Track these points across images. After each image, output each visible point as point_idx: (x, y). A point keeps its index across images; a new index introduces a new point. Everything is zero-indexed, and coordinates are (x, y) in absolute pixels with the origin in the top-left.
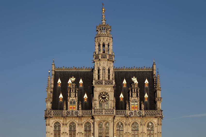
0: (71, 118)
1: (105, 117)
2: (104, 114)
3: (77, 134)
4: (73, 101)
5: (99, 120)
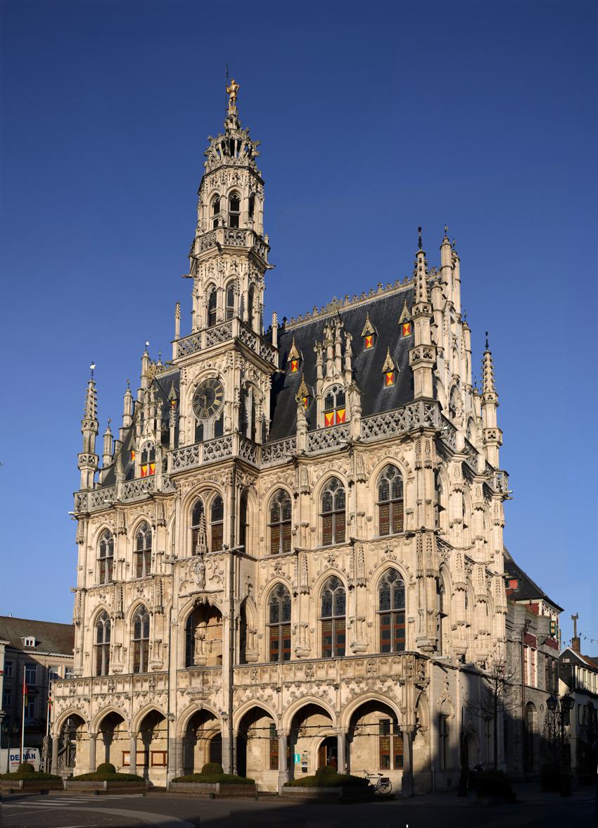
1: (207, 475)
2: (201, 462)
5: (188, 489)
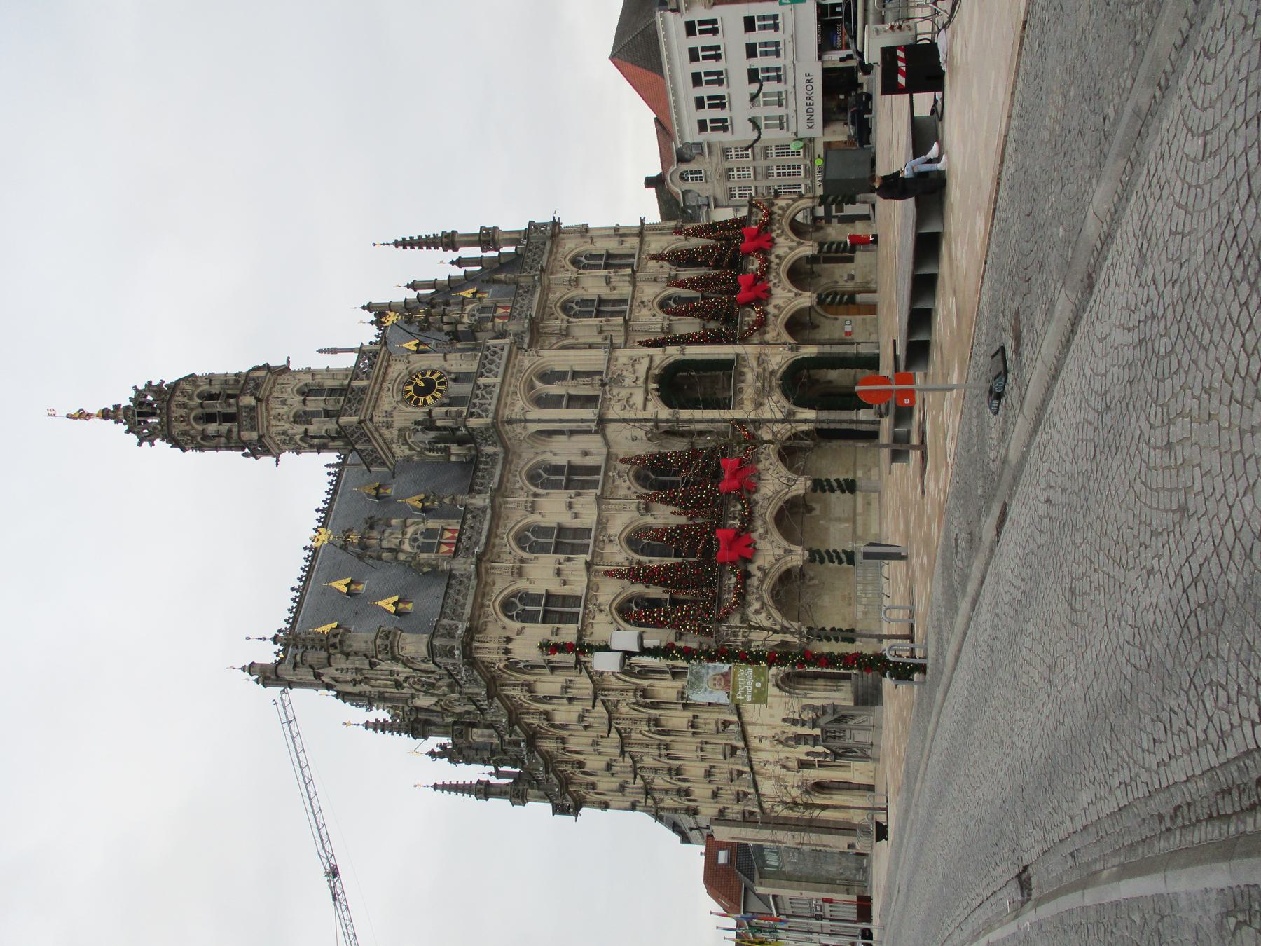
0: (497, 541)
2: (499, 380)
3: (576, 516)
4: (421, 539)
